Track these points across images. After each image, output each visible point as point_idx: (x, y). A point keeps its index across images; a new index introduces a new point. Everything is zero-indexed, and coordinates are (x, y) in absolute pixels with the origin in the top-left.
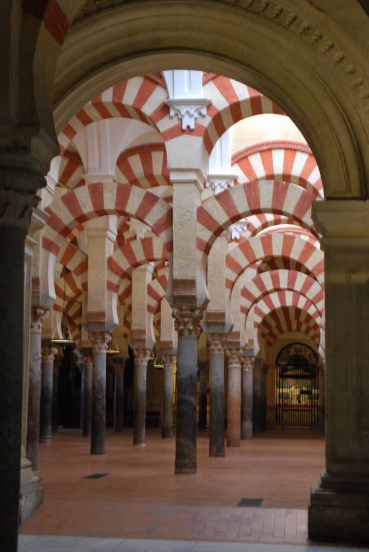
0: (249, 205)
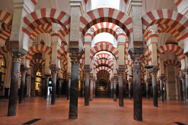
0: (100, 17)
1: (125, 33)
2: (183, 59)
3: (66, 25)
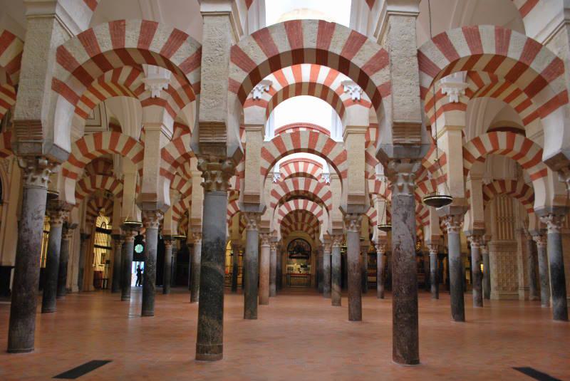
0: (291, 46)
1: (366, 98)
2: (541, 179)
3: (189, 72)
